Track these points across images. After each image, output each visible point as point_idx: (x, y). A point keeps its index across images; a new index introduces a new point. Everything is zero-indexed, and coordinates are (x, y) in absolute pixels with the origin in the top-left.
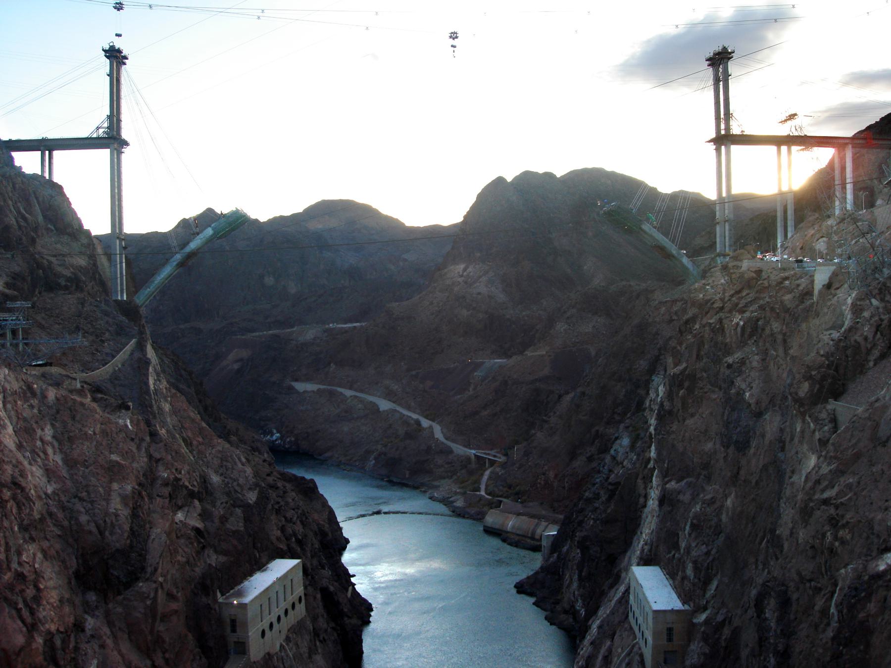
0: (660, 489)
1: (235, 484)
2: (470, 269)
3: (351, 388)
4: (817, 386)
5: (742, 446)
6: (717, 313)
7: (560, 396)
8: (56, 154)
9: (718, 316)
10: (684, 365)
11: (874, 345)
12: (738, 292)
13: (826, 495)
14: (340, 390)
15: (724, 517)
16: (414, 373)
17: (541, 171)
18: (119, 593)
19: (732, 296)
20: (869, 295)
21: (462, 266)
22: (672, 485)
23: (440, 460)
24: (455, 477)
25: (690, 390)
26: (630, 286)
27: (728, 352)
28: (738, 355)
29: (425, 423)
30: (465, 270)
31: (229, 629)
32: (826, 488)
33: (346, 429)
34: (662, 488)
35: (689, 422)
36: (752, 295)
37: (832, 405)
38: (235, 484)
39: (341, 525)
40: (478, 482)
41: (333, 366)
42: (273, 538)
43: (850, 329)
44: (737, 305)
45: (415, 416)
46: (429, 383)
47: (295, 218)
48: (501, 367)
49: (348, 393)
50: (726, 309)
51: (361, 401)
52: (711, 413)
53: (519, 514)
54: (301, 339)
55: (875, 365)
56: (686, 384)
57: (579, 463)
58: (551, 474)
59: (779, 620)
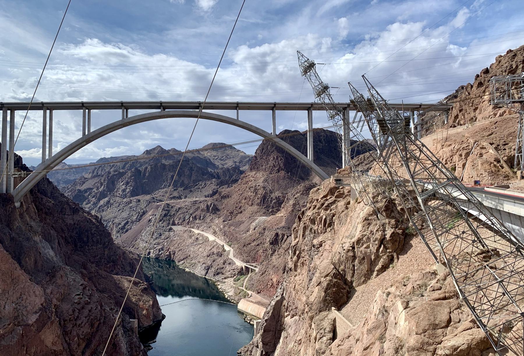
3: (198, 229)
4: (323, 294)
6: (314, 208)
7: (288, 237)
11: (378, 257)
12: (324, 197)
14: (193, 230)
16: (226, 223)
19: (322, 198)
20: (375, 212)
21: (254, 173)
23: (228, 268)
24: (235, 277)
25: (299, 257)
28: (320, 239)
29: (227, 248)
30: (255, 174)
33: (192, 249)
36: (333, 198)
37: (334, 313)
38: (25, 309)
39: (161, 308)
40: (244, 280)
41: (191, 219)
42: (49, 345)
43: (359, 241)
44: (323, 204)
46: (233, 228)
47: (198, 151)
49: (196, 231)
50: (317, 208)
51: (202, 236)
54: (183, 205)
55: (377, 275)
56: (297, 252)
58: (275, 280)
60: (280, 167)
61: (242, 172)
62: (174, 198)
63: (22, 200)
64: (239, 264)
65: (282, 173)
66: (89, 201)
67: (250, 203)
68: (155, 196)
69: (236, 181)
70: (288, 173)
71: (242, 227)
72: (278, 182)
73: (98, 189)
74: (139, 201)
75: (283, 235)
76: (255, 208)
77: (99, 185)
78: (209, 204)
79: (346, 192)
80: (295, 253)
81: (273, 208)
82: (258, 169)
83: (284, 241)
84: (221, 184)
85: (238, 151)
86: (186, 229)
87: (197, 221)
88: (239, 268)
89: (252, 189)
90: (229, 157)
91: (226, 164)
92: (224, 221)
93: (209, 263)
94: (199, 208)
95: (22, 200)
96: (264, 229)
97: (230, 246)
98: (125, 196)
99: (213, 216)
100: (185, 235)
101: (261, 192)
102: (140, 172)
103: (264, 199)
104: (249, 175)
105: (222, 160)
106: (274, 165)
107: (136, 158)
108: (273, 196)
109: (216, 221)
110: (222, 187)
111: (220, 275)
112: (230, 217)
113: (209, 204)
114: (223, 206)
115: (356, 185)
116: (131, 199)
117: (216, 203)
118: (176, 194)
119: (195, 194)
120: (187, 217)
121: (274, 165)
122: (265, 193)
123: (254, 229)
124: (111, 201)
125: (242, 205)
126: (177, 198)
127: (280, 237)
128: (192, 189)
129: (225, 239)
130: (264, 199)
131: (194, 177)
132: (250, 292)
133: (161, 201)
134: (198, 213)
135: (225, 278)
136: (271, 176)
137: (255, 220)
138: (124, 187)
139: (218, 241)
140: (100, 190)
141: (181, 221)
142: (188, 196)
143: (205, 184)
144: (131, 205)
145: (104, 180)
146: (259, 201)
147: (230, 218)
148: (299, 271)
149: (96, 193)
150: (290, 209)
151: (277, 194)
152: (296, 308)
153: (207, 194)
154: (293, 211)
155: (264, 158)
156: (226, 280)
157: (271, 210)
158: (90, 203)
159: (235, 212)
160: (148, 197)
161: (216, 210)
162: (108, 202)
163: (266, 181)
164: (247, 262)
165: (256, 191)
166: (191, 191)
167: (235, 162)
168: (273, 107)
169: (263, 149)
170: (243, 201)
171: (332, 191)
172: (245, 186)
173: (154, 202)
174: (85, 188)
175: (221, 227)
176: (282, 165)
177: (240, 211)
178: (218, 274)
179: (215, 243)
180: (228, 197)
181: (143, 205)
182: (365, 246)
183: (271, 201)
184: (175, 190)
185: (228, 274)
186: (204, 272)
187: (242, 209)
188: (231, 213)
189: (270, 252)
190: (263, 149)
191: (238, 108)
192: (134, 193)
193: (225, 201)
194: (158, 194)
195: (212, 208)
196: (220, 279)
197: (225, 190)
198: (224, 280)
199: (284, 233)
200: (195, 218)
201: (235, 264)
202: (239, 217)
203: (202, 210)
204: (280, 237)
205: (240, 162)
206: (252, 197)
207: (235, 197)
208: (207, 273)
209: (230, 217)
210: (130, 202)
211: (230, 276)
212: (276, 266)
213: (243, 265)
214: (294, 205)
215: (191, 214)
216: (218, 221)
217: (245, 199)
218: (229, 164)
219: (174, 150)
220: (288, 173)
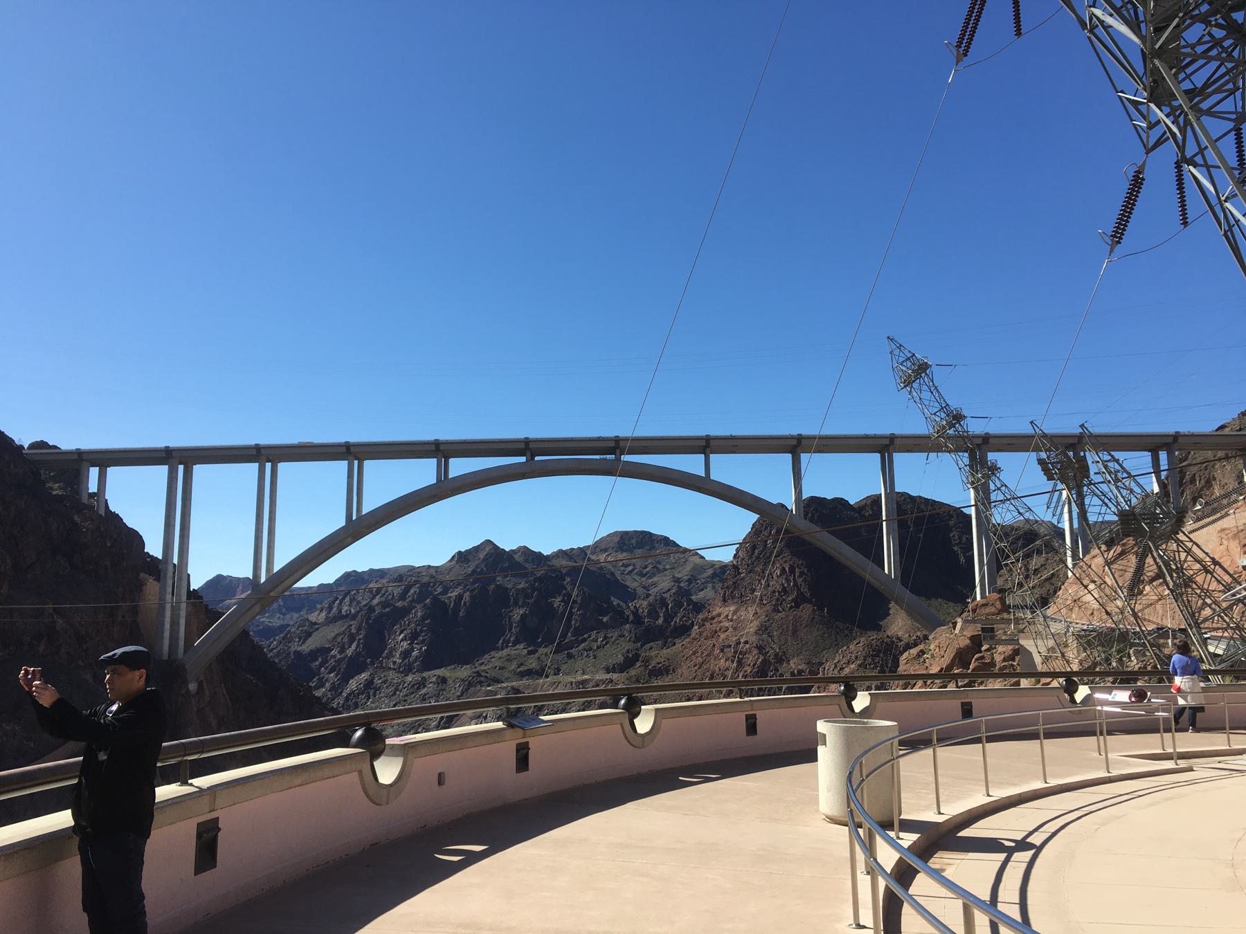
2: (742, 613)
8: (112, 471)
17: (829, 497)
21: (732, 608)
30: (735, 613)
47: (582, 551)
60: (800, 594)
61: (699, 607)
62: (529, 673)
63: (202, 678)
66: (320, 680)
68: (483, 667)
69: (684, 630)
72: (795, 632)
73: (342, 650)
74: (443, 680)
77: (346, 640)
79: (998, 658)
82: (742, 601)
84: (649, 635)
85: (686, 551)
89: (730, 652)
90: (661, 567)
91: (654, 585)
95: (202, 678)
98: (408, 670)
101: (753, 658)
102: (444, 606)
104: (719, 615)
105: (642, 575)
106: (784, 589)
107: (432, 572)
110: (648, 646)
115: (1039, 642)
116: (425, 674)
118: (532, 663)
119: (580, 663)
121: (784, 589)
122: (764, 661)
124: (377, 681)
128: (573, 651)
133: (498, 681)
138: (405, 644)
140: (349, 652)
142: (564, 667)
143: (605, 638)
144: (424, 691)
145: (359, 629)
149: (339, 662)
153: (611, 662)
155: (758, 569)
158: (323, 686)
160: (464, 672)
162: (369, 684)
163: (763, 629)
166: (570, 656)
167: (678, 580)
168: (795, 446)
169: (754, 548)
171: (962, 657)
172: (710, 642)
173: (481, 683)
174: (313, 647)
176: (804, 589)
181: (455, 690)
184: (530, 653)
191: (708, 450)
192: (429, 662)
194: (491, 662)
197: (658, 654)
205: (690, 581)
210: (422, 684)
218: (663, 583)
219: (525, 551)
220: (821, 609)
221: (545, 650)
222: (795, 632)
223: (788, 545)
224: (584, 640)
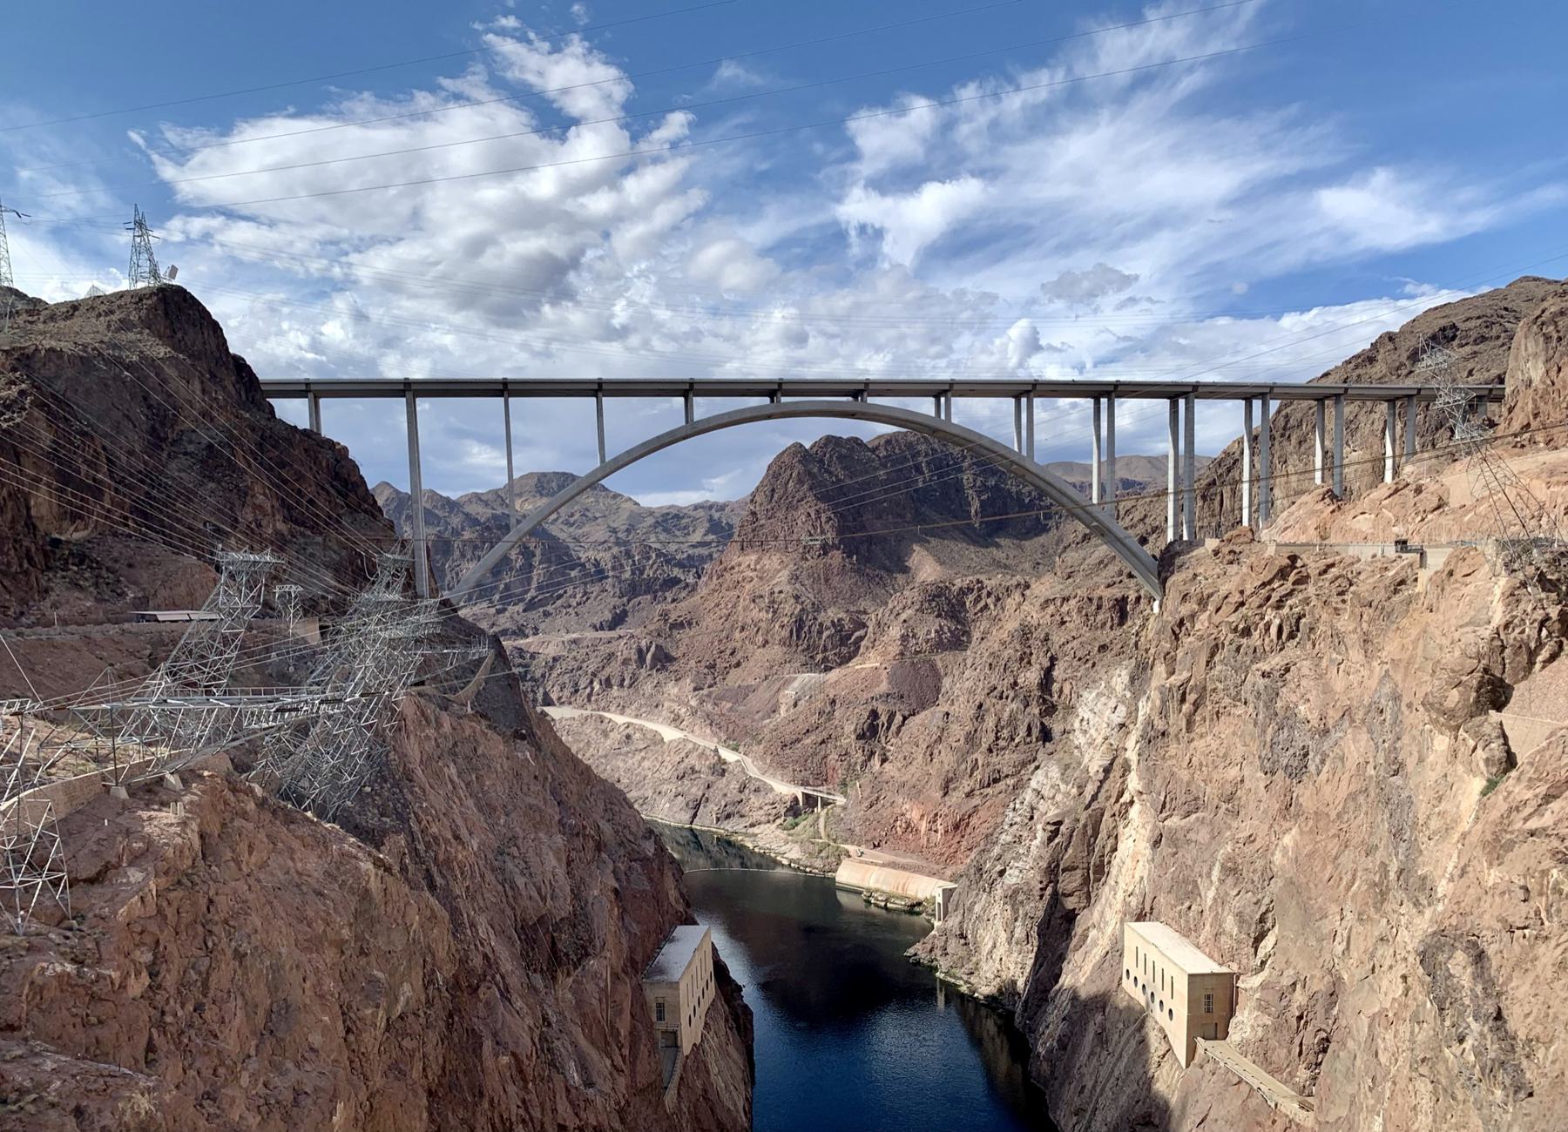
0: (1149, 827)
1: (627, 832)
2: (765, 561)
3: (622, 713)
5: (1297, 772)
7: (905, 718)
9: (1239, 614)
10: (1186, 675)
12: (1264, 585)
13: (1533, 824)
15: (1278, 858)
16: (705, 692)
18: (569, 975)
21: (754, 557)
22: (1174, 822)
23: (755, 801)
24: (778, 821)
26: (979, 581)
27: (1257, 654)
28: (1275, 662)
29: (729, 756)
30: (757, 562)
31: (654, 1017)
32: (1531, 815)
34: (1155, 826)
35: (1199, 744)
41: (596, 686)
42: (672, 900)
45: (711, 744)
48: (822, 686)
49: (620, 719)
52: (1234, 733)
53: (883, 865)
56: (1191, 698)
57: (956, 797)
59: (1476, 977)
64: (785, 790)
65: (836, 557)
67: (760, 639)
70: (850, 556)
71: (755, 701)
75: (892, 716)
76: (776, 651)
78: (643, 644)
80: (1183, 700)
81: (825, 650)
83: (894, 728)
84: (632, 590)
86: (588, 712)
87: (615, 691)
88: (788, 799)
92: (695, 689)
93: (696, 791)
94: (611, 656)
96: (833, 702)
97: (736, 749)
99: (658, 677)
100: (588, 729)
101: (789, 608)
103: (800, 629)
108: (821, 617)
109: (672, 689)
110: (636, 601)
111: (736, 819)
112: (710, 677)
113: (643, 644)
114: (683, 649)
117: (661, 641)
119: (560, 621)
120: (583, 683)
122: (803, 610)
123: (795, 705)
125: (738, 645)
126: (514, 633)
127: (883, 719)
128: (549, 608)
129: (715, 734)
130: (800, 629)
131: (538, 574)
132: (851, 848)
134: (613, 669)
135: (752, 825)
136: (806, 565)
137: (787, 683)
139: (691, 737)
141: (567, 693)
142: (542, 626)
143: (585, 593)
146: (785, 633)
147: (709, 680)
148: (1198, 730)
150: (895, 649)
151: (832, 614)
152: (1196, 799)
153: (596, 620)
154: (902, 654)
155: (780, 515)
156: (755, 830)
157: (820, 657)
159: (720, 664)
161: (663, 660)
163: (795, 578)
164: (805, 783)
165: (774, 607)
166: (546, 614)
167: (614, 531)
169: (773, 490)
170: (737, 635)
172: (731, 593)
175: (693, 703)
177: (734, 661)
178: (728, 817)
179: (690, 746)
180: (690, 624)
182: (1518, 630)
183: (820, 633)
185: (757, 815)
186: (686, 817)
187: (739, 656)
188: (712, 666)
189: (859, 757)
190: (773, 490)
193: (683, 635)
195: (654, 656)
196: (739, 828)
198: (751, 830)
199: (893, 708)
200: (608, 683)
201: (772, 789)
202: (735, 678)
203: (625, 662)
204: (883, 719)
206: (763, 625)
207: (710, 622)
208: (695, 815)
209: (710, 677)
211: (764, 819)
212: (909, 784)
213: (799, 792)
214: (904, 638)
215: (594, 675)
216: (678, 691)
217: (743, 629)
220: (850, 556)
221: (517, 608)
222: (827, 581)
223: (811, 489)
224: (560, 597)
